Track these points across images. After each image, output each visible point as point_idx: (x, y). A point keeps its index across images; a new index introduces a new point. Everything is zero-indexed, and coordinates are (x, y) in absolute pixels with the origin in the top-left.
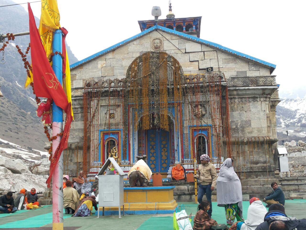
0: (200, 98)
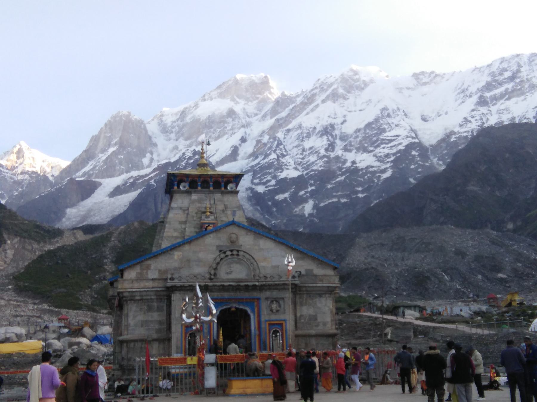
0: (275, 294)
